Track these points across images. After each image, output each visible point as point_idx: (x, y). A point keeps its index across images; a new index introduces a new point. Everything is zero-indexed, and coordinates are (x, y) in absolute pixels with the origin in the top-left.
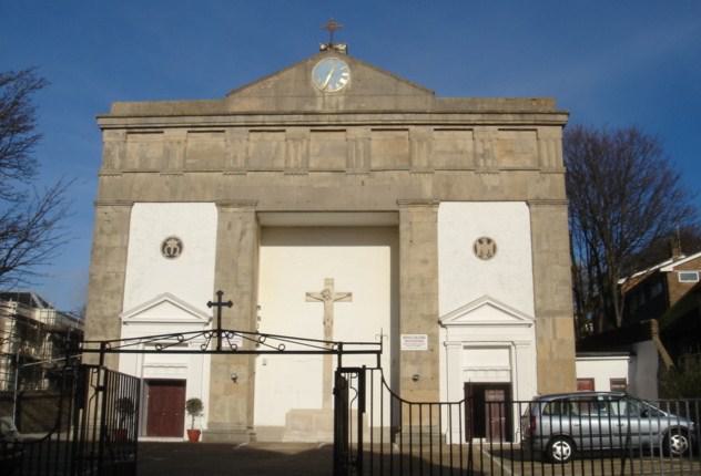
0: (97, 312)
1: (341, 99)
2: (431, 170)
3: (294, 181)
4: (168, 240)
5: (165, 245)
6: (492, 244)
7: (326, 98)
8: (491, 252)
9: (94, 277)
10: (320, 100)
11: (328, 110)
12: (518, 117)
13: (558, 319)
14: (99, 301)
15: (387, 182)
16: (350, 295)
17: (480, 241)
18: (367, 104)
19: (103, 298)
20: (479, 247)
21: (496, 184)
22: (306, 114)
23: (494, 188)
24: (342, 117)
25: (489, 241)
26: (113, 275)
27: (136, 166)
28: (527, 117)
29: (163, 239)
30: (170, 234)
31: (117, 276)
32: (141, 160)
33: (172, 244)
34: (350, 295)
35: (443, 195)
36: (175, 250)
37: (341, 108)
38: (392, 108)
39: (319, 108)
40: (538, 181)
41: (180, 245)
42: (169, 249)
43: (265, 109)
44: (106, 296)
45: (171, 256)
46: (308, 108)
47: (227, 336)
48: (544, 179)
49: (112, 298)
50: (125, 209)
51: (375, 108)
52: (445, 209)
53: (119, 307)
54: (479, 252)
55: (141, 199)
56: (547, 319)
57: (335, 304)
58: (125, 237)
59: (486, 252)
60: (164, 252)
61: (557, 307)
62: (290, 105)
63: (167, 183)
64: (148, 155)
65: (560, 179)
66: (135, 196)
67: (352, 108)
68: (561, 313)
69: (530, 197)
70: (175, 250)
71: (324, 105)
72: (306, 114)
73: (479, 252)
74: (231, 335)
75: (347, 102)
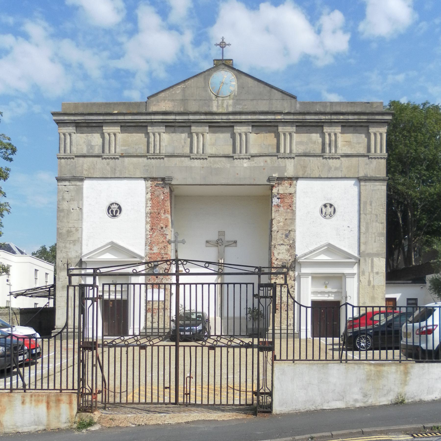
0: (64, 255)
1: (231, 102)
2: (293, 155)
3: (196, 163)
4: (111, 205)
5: (109, 208)
6: (332, 208)
7: (220, 102)
8: (332, 213)
9: (60, 231)
10: (215, 104)
11: (220, 110)
12: (356, 117)
13: (376, 260)
14: (65, 247)
15: (262, 164)
16: (235, 242)
17: (325, 206)
18: (249, 107)
19: (68, 245)
20: (324, 210)
21: (338, 165)
22: (206, 114)
23: (336, 169)
24: (231, 117)
25: (331, 205)
26: (73, 229)
27: (85, 151)
28: (362, 117)
29: (107, 204)
30: (113, 201)
31: (77, 230)
32: (87, 146)
33: (114, 207)
34: (235, 242)
35: (300, 174)
36: (116, 212)
37: (231, 109)
38: (265, 109)
39: (215, 109)
40: (367, 164)
41: (120, 208)
42: (112, 211)
43: (176, 110)
44: (70, 243)
45: (114, 216)
46: (205, 109)
47: (182, 264)
48: (371, 162)
49: (74, 245)
50: (78, 183)
51: (253, 110)
52: (301, 184)
53: (80, 252)
54: (324, 214)
55: (90, 176)
56: (367, 259)
57: (227, 249)
58: (81, 202)
59: (328, 213)
60: (109, 213)
61: (375, 251)
62: (193, 107)
63: (108, 164)
64: (93, 144)
65: (383, 162)
66: (85, 174)
67: (238, 109)
68: (377, 255)
69: (361, 174)
70: (116, 212)
71: (218, 106)
72: (206, 114)
73: (324, 214)
74: (185, 263)
75: (234, 105)
